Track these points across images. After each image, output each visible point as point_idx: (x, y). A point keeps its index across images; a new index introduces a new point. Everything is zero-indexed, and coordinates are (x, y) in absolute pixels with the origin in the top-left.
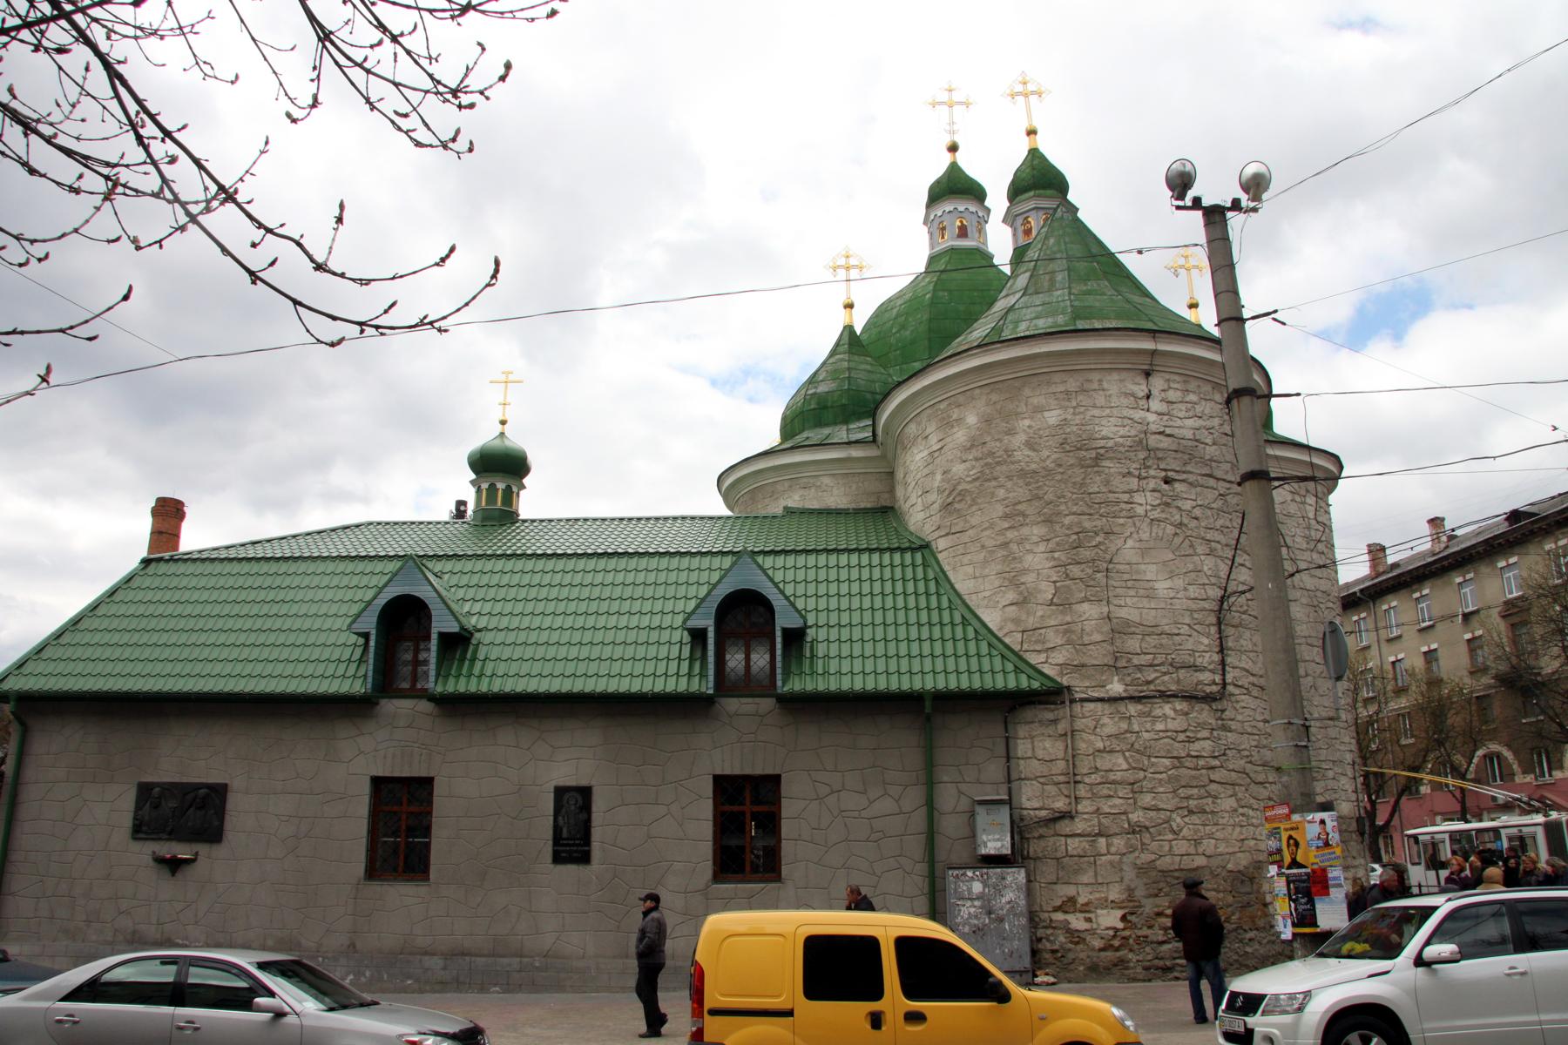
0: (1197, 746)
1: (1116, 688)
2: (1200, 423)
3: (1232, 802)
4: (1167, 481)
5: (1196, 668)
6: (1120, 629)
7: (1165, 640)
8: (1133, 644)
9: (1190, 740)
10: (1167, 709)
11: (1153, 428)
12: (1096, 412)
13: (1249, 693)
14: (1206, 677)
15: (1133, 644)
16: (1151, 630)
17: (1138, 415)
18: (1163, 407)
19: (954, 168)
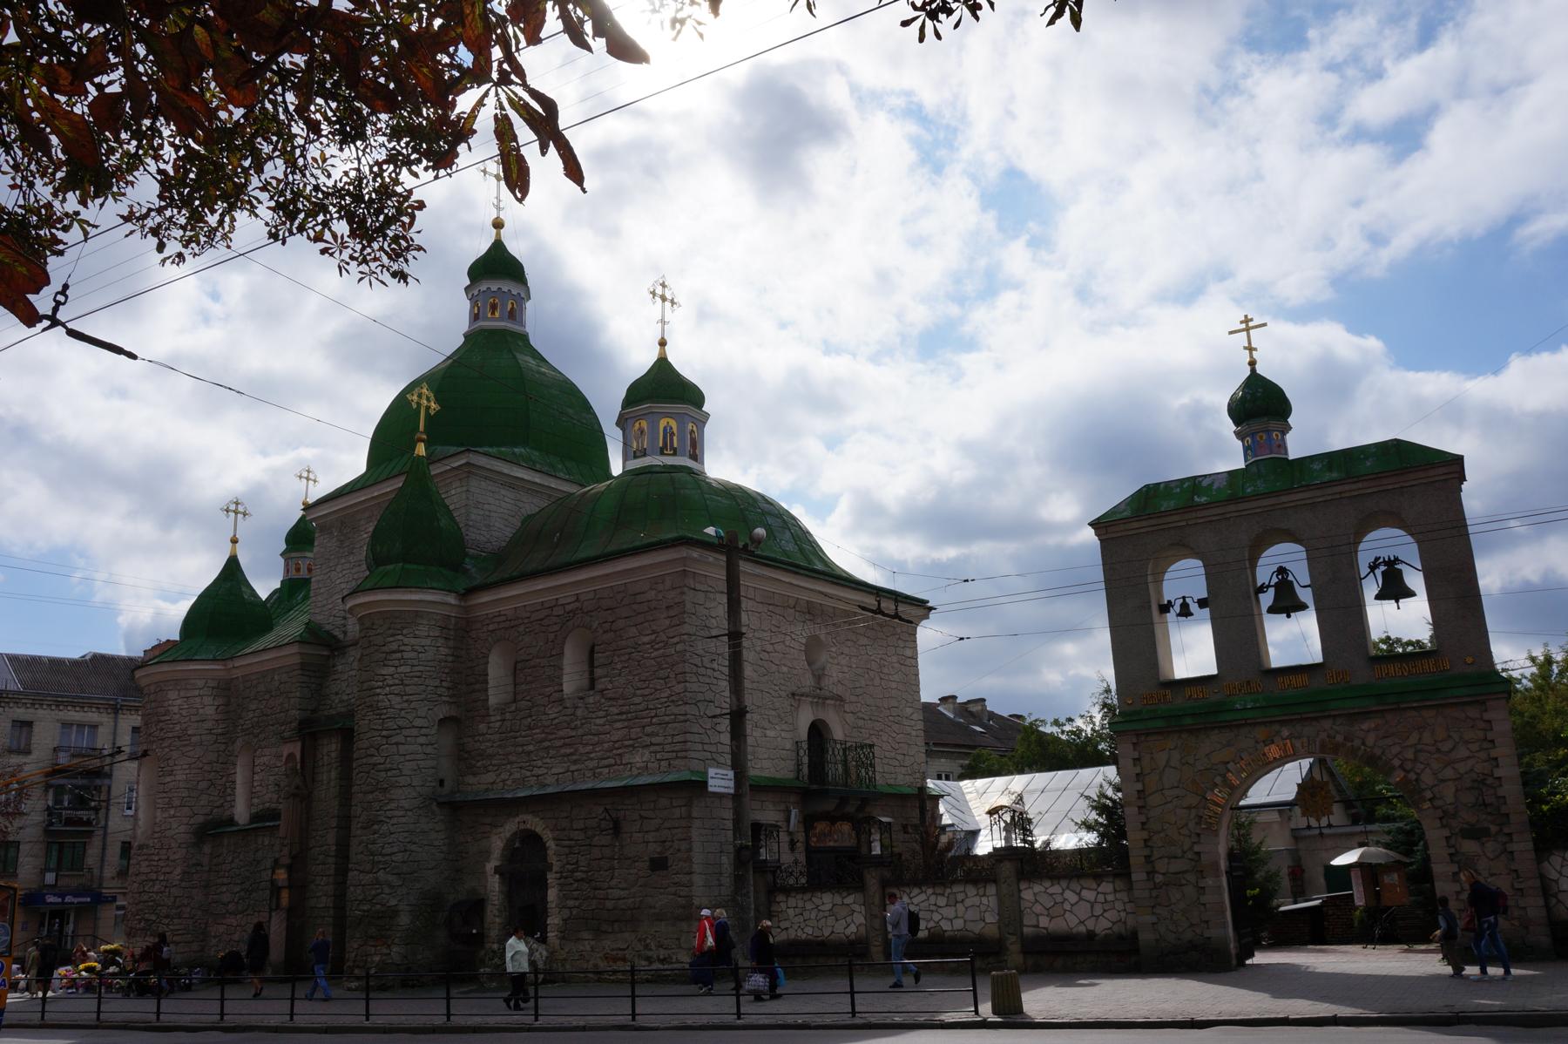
19: (498, 246)
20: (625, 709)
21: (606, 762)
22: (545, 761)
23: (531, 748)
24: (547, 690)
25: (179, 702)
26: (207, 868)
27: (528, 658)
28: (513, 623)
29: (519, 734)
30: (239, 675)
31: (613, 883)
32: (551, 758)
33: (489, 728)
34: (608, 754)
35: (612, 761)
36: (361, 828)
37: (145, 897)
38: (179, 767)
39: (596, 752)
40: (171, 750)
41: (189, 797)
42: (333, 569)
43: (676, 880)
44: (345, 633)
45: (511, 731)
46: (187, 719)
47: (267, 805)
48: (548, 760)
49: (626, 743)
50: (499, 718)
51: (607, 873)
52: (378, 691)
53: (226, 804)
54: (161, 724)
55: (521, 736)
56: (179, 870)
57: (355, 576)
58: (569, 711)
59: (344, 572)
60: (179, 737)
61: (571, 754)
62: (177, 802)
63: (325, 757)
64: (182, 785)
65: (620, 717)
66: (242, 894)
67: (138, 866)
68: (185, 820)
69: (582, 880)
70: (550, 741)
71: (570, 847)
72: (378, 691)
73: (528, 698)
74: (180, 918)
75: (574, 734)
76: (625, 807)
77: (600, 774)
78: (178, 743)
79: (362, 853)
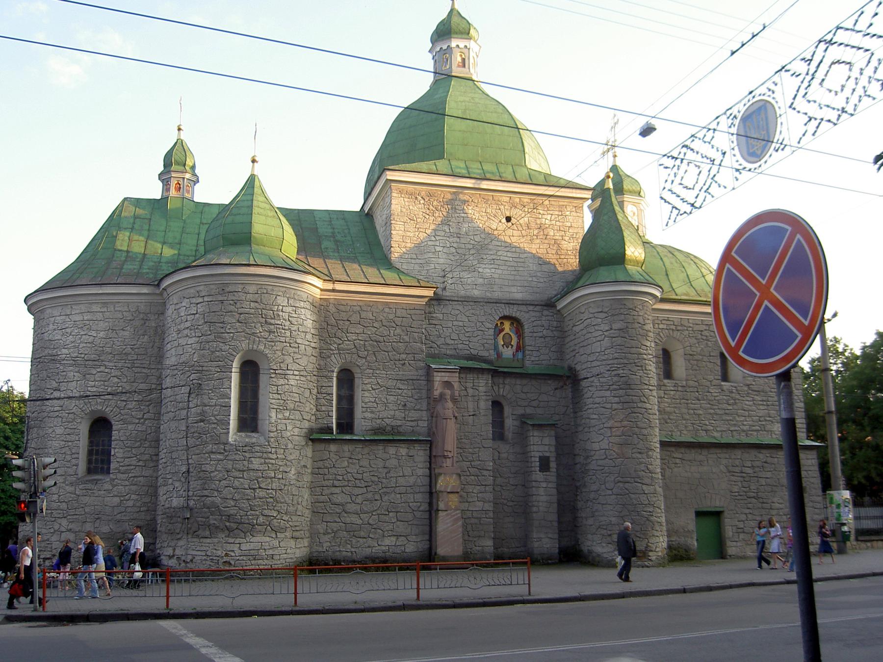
20: (764, 398)
21: (754, 428)
22: (710, 421)
23: (701, 412)
24: (708, 377)
25: (290, 309)
26: (309, 471)
27: (691, 353)
28: (679, 328)
29: (689, 401)
30: (332, 297)
31: (775, 500)
32: (715, 420)
33: (665, 393)
34: (756, 424)
35: (758, 428)
36: (640, 453)
37: (262, 493)
38: (291, 372)
39: (746, 421)
40: (283, 354)
41: (300, 402)
42: (421, 230)
43: (813, 499)
44: (445, 289)
45: (683, 399)
46: (295, 328)
48: (714, 422)
49: (768, 419)
50: (672, 389)
51: (770, 494)
52: (645, 356)
53: (318, 413)
54: (272, 327)
55: (692, 404)
56: (293, 472)
57: (455, 245)
58: (727, 393)
59: (438, 238)
60: (290, 343)
61: (731, 420)
62: (291, 405)
63: (470, 391)
64: (294, 389)
65: (761, 403)
66: (370, 496)
67: (246, 463)
68: (298, 424)
69: (754, 497)
70: (714, 409)
71: (744, 477)
72: (645, 356)
73: (696, 380)
74: (296, 515)
75: (731, 408)
76: (778, 456)
77: (751, 434)
78: (291, 350)
79: (643, 471)
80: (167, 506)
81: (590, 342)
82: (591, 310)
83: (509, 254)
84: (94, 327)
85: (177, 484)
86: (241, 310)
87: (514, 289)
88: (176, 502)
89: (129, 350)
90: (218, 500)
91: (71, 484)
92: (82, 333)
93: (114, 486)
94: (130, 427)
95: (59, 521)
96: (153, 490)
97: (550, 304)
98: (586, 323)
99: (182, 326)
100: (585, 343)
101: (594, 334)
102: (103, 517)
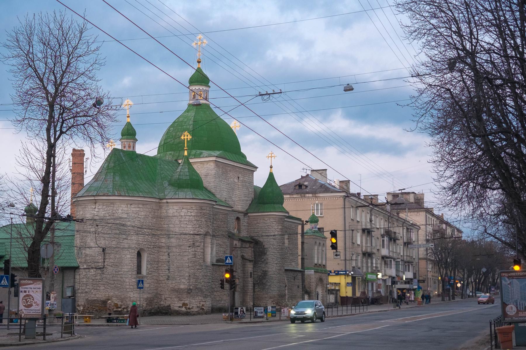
0: (97, 277)
1: (85, 266)
2: (106, 212)
3: (104, 288)
4: (97, 226)
5: (98, 262)
6: (86, 255)
7: (93, 257)
8: (88, 258)
9: (96, 276)
10: (92, 270)
11: (95, 215)
12: (86, 212)
13: (112, 267)
14: (100, 264)
15: (88, 258)
16: (91, 256)
17: (93, 212)
18: (98, 210)
47: (221, 257)
80: (176, 287)
81: (269, 232)
82: (271, 220)
83: (240, 193)
84: (140, 214)
85: (183, 280)
86: (206, 217)
87: (239, 207)
88: (182, 287)
89: (150, 225)
90: (200, 286)
91: (134, 278)
92: (136, 216)
93: (147, 279)
94: (152, 256)
95: (130, 293)
96: (158, 281)
97: (246, 214)
98: (267, 224)
99: (183, 219)
100: (266, 232)
101: (272, 229)
102: (145, 292)
